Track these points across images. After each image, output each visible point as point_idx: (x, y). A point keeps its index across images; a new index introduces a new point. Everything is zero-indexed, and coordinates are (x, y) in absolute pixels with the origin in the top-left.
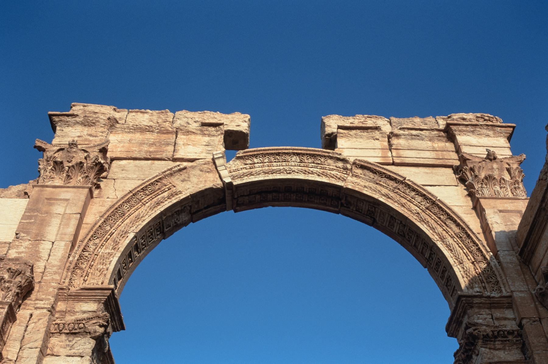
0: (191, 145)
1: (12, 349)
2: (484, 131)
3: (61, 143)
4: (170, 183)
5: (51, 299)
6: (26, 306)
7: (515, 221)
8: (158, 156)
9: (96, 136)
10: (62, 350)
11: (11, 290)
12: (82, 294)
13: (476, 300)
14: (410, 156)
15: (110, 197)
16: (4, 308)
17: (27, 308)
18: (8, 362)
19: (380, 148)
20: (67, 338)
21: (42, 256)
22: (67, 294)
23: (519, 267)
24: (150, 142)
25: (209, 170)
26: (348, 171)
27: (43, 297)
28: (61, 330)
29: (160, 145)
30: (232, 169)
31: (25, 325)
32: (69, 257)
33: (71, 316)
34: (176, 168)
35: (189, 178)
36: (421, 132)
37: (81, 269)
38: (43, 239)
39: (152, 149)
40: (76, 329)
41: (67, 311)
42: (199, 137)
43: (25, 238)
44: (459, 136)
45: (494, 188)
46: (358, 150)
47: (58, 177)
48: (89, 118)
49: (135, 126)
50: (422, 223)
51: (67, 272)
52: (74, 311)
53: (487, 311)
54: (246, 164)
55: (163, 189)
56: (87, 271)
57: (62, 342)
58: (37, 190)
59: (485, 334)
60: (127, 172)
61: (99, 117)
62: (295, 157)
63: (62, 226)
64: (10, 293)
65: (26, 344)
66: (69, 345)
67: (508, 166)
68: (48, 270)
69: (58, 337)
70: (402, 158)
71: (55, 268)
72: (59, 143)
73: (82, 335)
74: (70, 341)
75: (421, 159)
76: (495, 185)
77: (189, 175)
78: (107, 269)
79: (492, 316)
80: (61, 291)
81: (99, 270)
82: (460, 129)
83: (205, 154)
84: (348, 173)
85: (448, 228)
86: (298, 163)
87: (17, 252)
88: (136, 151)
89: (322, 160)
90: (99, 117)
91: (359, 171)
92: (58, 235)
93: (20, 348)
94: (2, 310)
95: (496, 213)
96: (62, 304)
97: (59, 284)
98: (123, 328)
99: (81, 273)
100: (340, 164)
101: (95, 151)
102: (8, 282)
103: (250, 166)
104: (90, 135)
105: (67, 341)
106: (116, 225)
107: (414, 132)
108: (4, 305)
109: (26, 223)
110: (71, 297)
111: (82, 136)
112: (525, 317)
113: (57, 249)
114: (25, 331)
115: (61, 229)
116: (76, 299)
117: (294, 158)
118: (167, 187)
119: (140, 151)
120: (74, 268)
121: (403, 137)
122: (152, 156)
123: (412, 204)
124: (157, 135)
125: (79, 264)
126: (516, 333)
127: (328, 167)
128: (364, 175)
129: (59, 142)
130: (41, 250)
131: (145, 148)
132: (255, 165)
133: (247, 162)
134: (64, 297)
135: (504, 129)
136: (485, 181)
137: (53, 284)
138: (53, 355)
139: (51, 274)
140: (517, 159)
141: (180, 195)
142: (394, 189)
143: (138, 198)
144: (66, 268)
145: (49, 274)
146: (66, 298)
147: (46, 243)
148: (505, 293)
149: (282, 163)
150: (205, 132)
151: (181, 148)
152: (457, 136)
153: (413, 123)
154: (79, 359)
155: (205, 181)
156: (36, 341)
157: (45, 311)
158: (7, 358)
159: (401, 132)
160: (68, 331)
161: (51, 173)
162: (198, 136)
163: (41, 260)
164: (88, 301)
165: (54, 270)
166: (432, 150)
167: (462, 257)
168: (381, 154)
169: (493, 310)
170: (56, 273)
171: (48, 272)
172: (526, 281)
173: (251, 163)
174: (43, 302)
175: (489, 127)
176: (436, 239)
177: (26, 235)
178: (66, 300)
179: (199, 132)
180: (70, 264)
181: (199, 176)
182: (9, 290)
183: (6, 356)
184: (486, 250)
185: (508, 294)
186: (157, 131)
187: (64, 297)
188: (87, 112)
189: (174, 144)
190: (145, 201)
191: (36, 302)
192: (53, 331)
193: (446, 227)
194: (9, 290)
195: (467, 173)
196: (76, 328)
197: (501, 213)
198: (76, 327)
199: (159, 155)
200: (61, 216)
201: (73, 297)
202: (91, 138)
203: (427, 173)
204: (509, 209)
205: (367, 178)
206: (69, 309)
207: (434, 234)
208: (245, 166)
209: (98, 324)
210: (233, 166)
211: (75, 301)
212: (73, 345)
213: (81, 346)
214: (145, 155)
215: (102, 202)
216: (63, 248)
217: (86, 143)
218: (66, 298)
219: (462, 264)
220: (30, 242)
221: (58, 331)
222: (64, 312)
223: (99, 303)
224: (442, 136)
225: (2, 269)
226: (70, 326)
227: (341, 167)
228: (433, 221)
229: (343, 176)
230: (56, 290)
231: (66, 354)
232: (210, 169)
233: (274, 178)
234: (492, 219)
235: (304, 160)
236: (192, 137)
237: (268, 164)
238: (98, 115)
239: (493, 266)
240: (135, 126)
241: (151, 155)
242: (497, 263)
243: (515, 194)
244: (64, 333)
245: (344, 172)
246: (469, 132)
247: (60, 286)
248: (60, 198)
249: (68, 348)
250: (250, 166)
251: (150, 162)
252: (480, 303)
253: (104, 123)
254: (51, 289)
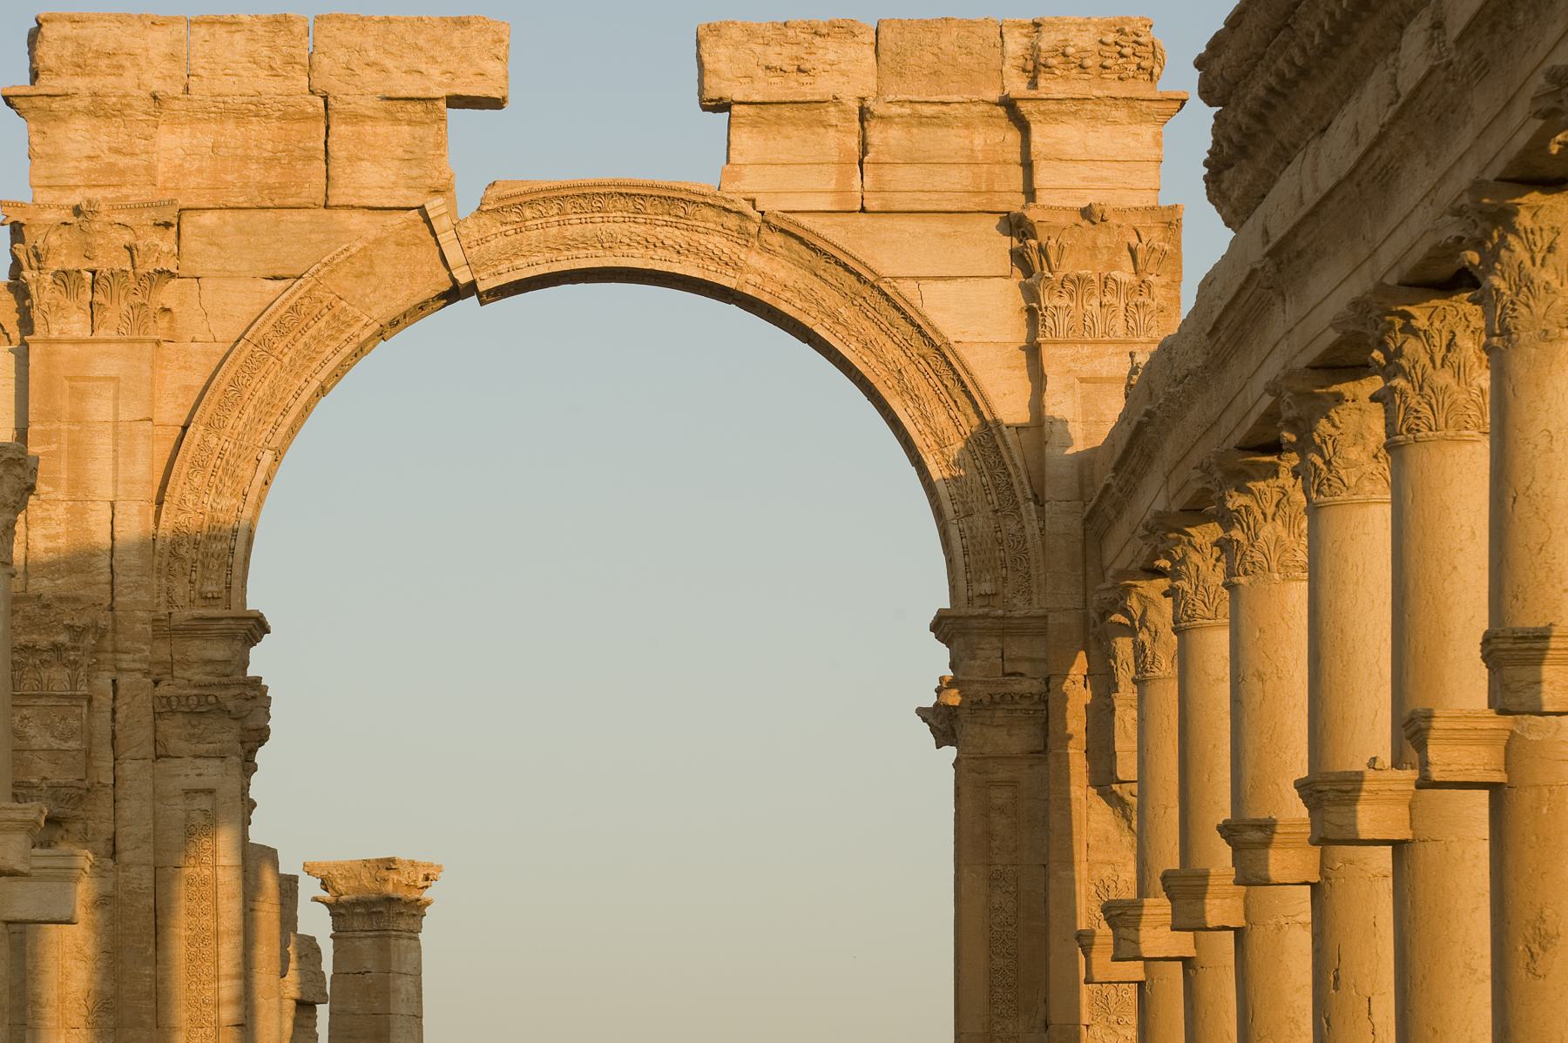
0: (368, 160)
1: (102, 764)
2: (1102, 110)
3: (52, 182)
4: (332, 292)
5: (142, 651)
7: (1107, 412)
8: (291, 201)
9: (133, 154)
10: (183, 745)
13: (974, 623)
14: (906, 183)
15: (199, 337)
16: (81, 706)
19: (836, 159)
20: (186, 721)
23: (1080, 546)
24: (265, 154)
25: (417, 241)
26: (752, 240)
27: (128, 644)
29: (289, 163)
30: (473, 238)
31: (109, 709)
33: (185, 670)
34: (342, 256)
35: (371, 267)
36: (944, 108)
39: (271, 181)
42: (384, 129)
43: (53, 496)
44: (1040, 124)
45: (1086, 307)
46: (779, 167)
47: (75, 305)
48: (106, 100)
49: (222, 105)
50: (906, 397)
51: (159, 577)
53: (995, 640)
54: (503, 223)
55: (316, 312)
58: (38, 351)
59: (975, 699)
60: (223, 254)
61: (128, 95)
62: (623, 201)
63: (121, 460)
64: (81, 669)
66: (194, 735)
67: (1134, 240)
70: (886, 195)
71: (134, 573)
72: (45, 182)
74: (194, 727)
75: (936, 196)
76: (1092, 294)
77: (372, 261)
78: (232, 550)
79: (1003, 653)
80: (156, 623)
81: (216, 556)
82: (1042, 108)
83: (405, 192)
84: (750, 244)
85: (958, 414)
86: (630, 215)
87: (46, 537)
88: (234, 185)
89: (690, 209)
90: (128, 95)
91: (776, 240)
92: (120, 487)
93: (115, 760)
94: (78, 711)
95: (1072, 387)
96: (161, 645)
100: (732, 222)
101: (147, 225)
102: (73, 648)
103: (514, 227)
104: (118, 151)
106: (229, 428)
107: (928, 110)
111: (98, 156)
112: (1056, 672)
113: (127, 523)
114: (114, 720)
115: (121, 467)
117: (621, 203)
118: (325, 304)
119: (246, 184)
121: (897, 120)
122: (277, 202)
123: (889, 344)
124: (278, 124)
126: (1036, 697)
127: (703, 224)
128: (788, 249)
129: (47, 178)
130: (93, 528)
131: (254, 172)
132: (528, 223)
133: (509, 219)
135: (1155, 105)
136: (1069, 286)
137: (139, 614)
139: (129, 590)
140: (1163, 215)
141: (355, 329)
142: (853, 296)
143: (265, 349)
145: (126, 588)
147: (99, 507)
148: (1036, 611)
149: (592, 215)
150: (399, 115)
151: (343, 172)
152: (1032, 126)
153: (936, 51)
154: (218, 762)
155: (412, 276)
157: (139, 676)
158: (99, 783)
159: (895, 110)
161: (57, 294)
162: (381, 123)
165: (134, 579)
166: (965, 161)
167: (975, 499)
168: (834, 181)
169: (1008, 639)
170: (139, 585)
171: (121, 583)
172: (1085, 580)
173: (518, 220)
175: (1118, 102)
176: (926, 449)
177: (51, 489)
179: (383, 114)
181: (396, 258)
184: (1023, 490)
185: (1041, 612)
186: (277, 114)
188: (90, 55)
189: (323, 157)
190: (281, 352)
191: (119, 656)
193: (955, 409)
195: (1031, 255)
197: (1084, 385)
199: (292, 196)
200: (109, 426)
202: (123, 162)
203: (943, 235)
204: (1104, 375)
205: (795, 256)
207: (927, 430)
208: (504, 228)
210: (476, 229)
214: (259, 199)
215: (184, 357)
216: (137, 519)
217: (115, 180)
219: (971, 519)
220: (64, 504)
222: (166, 662)
223: (233, 640)
224: (998, 117)
226: (191, 702)
227: (733, 228)
228: (931, 389)
229: (734, 257)
230: (150, 629)
232: (419, 238)
233: (573, 268)
234: (1056, 408)
235: (645, 209)
236: (368, 128)
237: (557, 218)
238: (116, 58)
239: (1029, 537)
240: (222, 105)
241: (273, 196)
242: (1037, 532)
243: (1132, 323)
245: (739, 241)
246: (1067, 114)
248: (97, 374)
249: (194, 741)
250: (514, 227)
251: (269, 214)
252: (981, 629)
253: (145, 108)
254: (139, 627)
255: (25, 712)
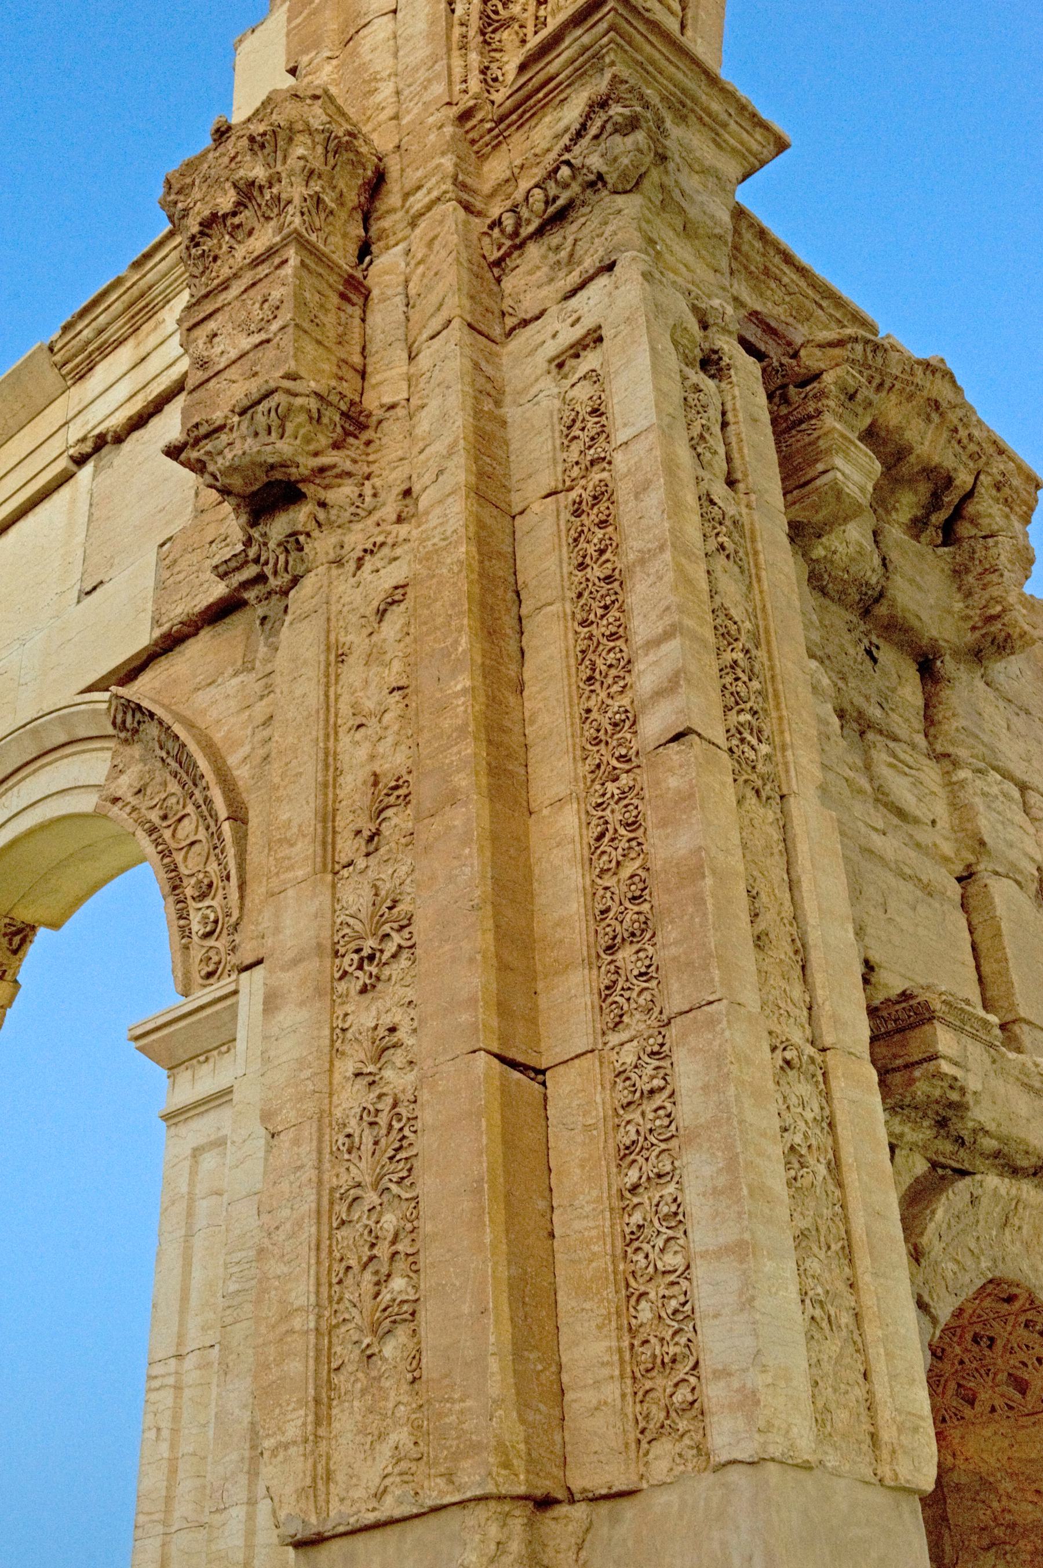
6: (387, 237)
11: (289, 202)
12: (530, 85)
17: (392, 241)
18: (387, 415)
21: (378, 68)
22: (492, 120)
27: (420, 173)
28: (516, 234)
32: (453, 11)
37: (505, 24)
38: (363, 22)
40: (556, 198)
41: (516, 171)
52: (536, 155)
56: (537, 18)
57: (538, 268)
64: (290, 209)
65: (420, 333)
68: (406, 93)
69: (518, 261)
73: (584, 204)
74: (558, 248)
80: (470, 124)
97: (449, 104)
98: (782, 146)
99: (517, 33)
105: (551, 254)
108: (282, 252)
109: (304, 21)
110: (507, 122)
116: (528, 115)
120: (483, 34)
125: (496, 12)
134: (487, 138)
137: (431, 120)
138: (525, 323)
144: (455, 46)
146: (497, 136)
154: (603, 280)
156: (441, 305)
158: (382, 406)
160: (535, 224)
163: (379, 85)
164: (562, 97)
174: (424, 190)
178: (500, 142)
180: (464, 29)
182: (282, 204)
183: (377, 404)
187: (487, 138)
192: (497, 255)
194: (282, 204)
196: (552, 193)
198: (553, 189)
201: (514, 117)
206: (518, 162)
209: (609, 127)
211: (527, 126)
212: (571, 255)
213: (596, 240)
218: (497, 136)
220: (334, 62)
221: (508, 243)
222: (507, 181)
225: (238, 159)
230: (449, 130)
231: (560, 296)
244: (530, 237)
247: (454, 111)
255: (212, 325)
